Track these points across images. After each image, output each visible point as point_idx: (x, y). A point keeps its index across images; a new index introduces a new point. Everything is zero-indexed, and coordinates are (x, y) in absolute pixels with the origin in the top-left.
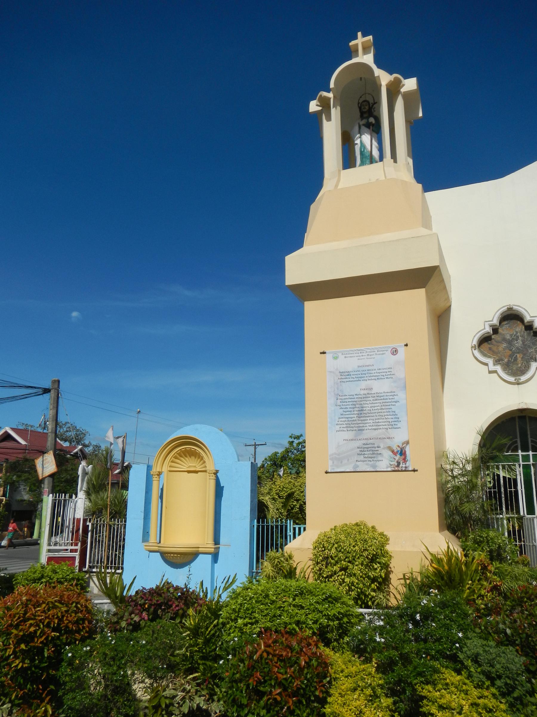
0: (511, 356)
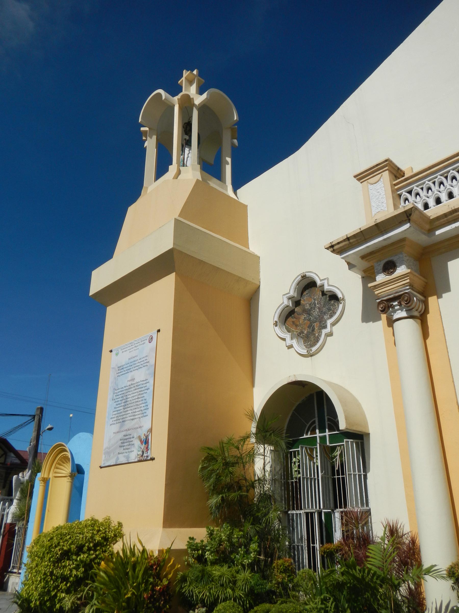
0: (309, 327)
